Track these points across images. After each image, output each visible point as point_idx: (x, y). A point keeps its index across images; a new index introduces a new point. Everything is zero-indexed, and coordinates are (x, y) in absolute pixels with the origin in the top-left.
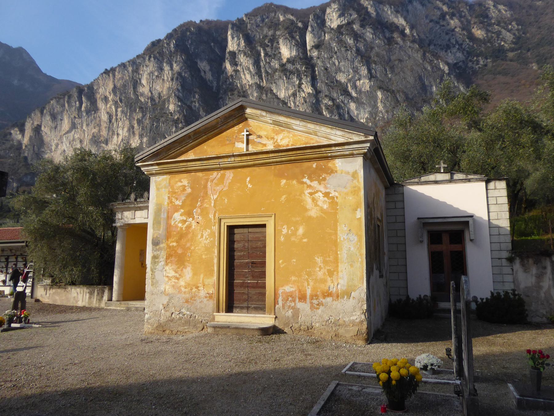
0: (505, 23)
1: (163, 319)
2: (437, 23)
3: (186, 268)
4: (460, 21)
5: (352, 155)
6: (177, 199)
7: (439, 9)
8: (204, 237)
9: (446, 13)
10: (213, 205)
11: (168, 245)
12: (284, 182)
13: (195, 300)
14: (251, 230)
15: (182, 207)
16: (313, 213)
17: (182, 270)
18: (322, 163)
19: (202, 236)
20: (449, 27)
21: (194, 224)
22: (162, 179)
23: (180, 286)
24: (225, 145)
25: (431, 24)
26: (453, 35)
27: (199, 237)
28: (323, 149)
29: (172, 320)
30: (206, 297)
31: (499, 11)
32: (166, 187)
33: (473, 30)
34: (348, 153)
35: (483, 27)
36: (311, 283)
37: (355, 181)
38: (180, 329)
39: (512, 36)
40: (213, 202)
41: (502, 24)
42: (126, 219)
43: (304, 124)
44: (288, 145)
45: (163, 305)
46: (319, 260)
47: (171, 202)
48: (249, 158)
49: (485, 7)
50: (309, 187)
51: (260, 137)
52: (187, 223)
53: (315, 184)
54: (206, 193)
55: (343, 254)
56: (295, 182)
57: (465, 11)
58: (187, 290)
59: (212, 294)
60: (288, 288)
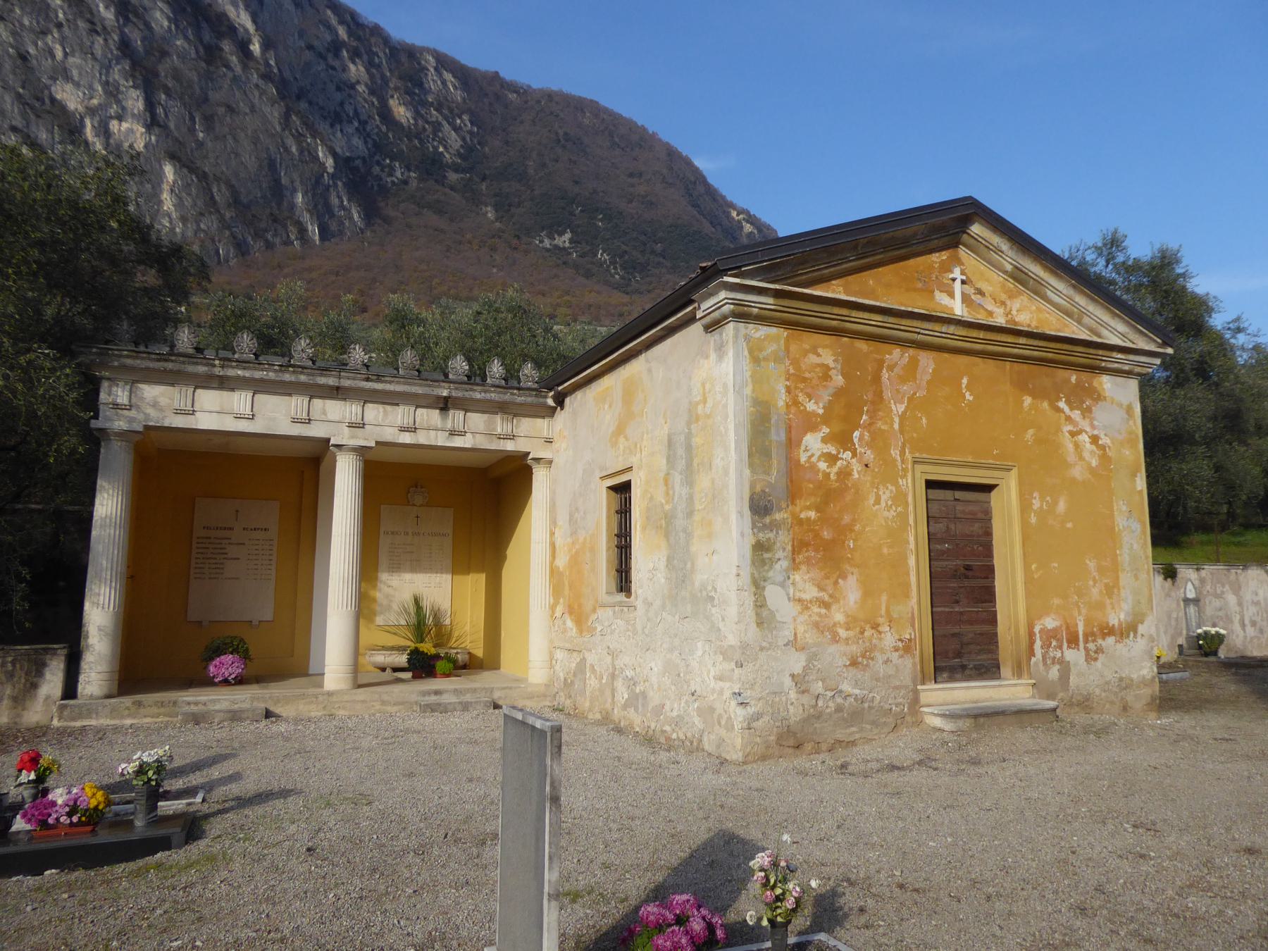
0: (451, 111)
1: (795, 714)
2: (322, 56)
3: (844, 577)
4: (367, 70)
5: (1128, 374)
6: (810, 397)
7: (329, 27)
8: (883, 504)
9: (343, 44)
10: (896, 426)
11: (795, 516)
12: (1028, 400)
13: (872, 659)
14: (958, 494)
15: (826, 419)
16: (1077, 472)
17: (836, 583)
18: (1085, 376)
19: (878, 502)
20: (344, 76)
21: (856, 467)
22: (767, 337)
23: (835, 625)
24: (915, 290)
25: (308, 55)
26: (350, 96)
27: (872, 502)
28: (1101, 352)
29: (819, 716)
30: (896, 650)
31: (444, 83)
32: (777, 360)
33: (391, 102)
34: (1127, 368)
35: (411, 103)
36: (1084, 611)
37: (1131, 423)
38: (840, 734)
39: (460, 143)
40: (897, 420)
41: (445, 111)
42: (151, 412)
43: (1071, 292)
44: (1029, 326)
45: (793, 676)
46: (1092, 565)
47: (796, 403)
48: (982, 334)
49: (419, 64)
50: (1068, 418)
51: (980, 292)
52: (839, 463)
53: (1076, 415)
54: (879, 395)
55: (1124, 557)
56: (1045, 404)
57: (382, 57)
58: (851, 633)
59: (910, 640)
60: (1050, 623)
